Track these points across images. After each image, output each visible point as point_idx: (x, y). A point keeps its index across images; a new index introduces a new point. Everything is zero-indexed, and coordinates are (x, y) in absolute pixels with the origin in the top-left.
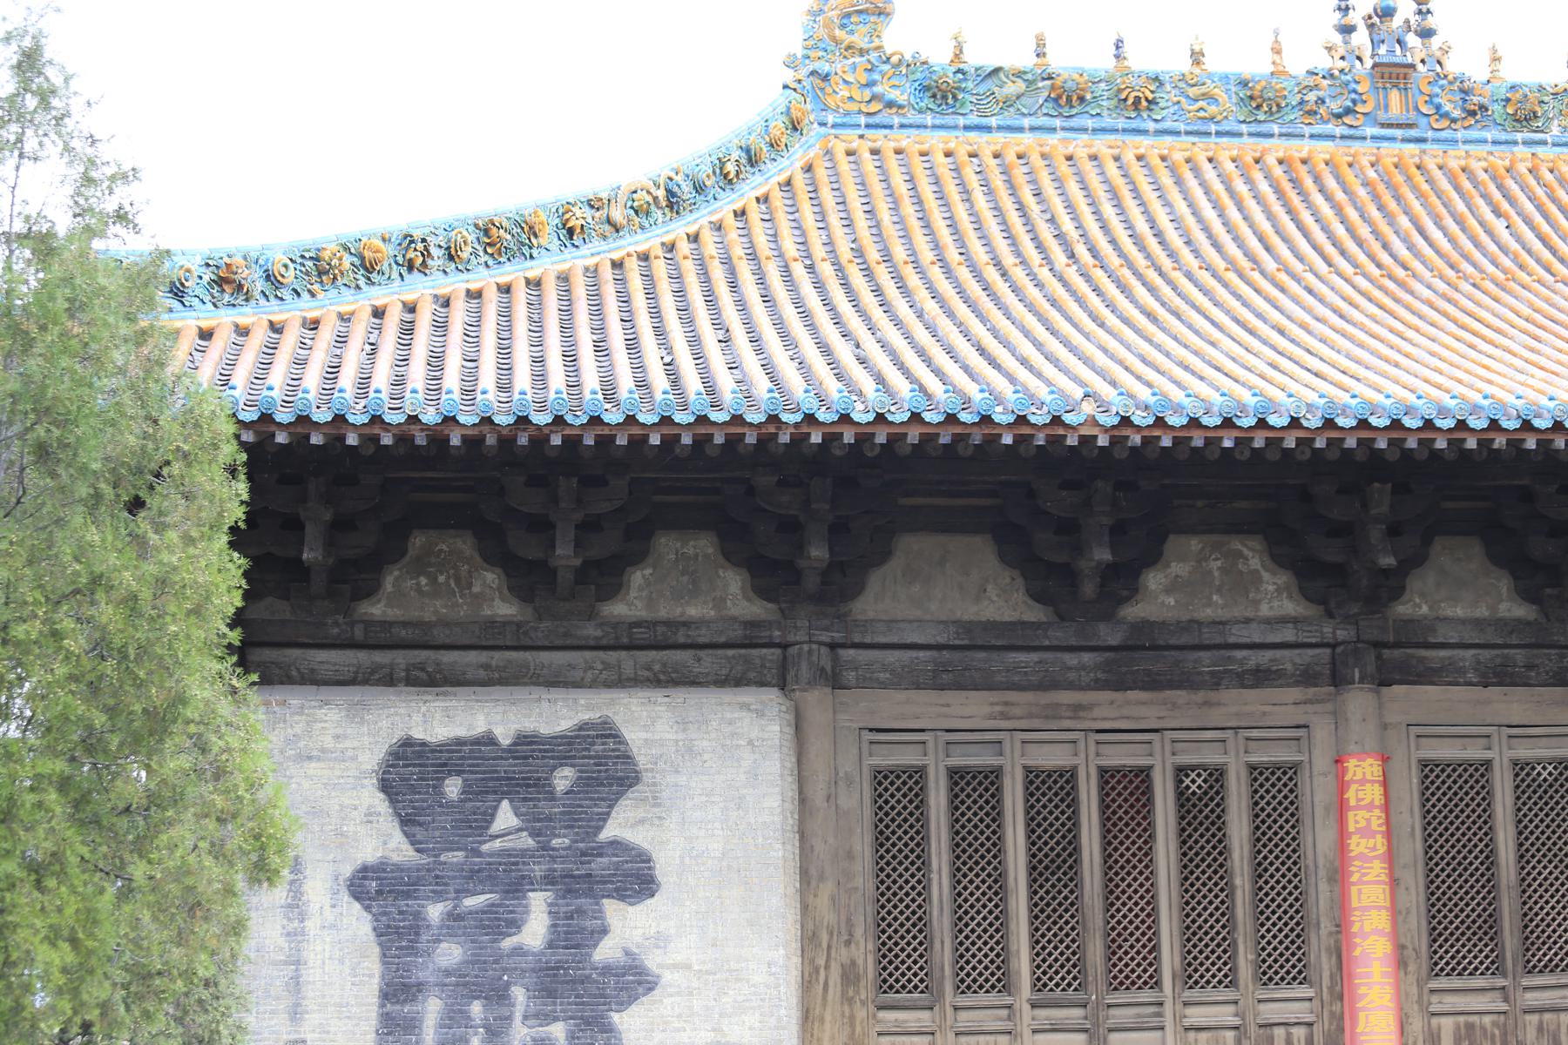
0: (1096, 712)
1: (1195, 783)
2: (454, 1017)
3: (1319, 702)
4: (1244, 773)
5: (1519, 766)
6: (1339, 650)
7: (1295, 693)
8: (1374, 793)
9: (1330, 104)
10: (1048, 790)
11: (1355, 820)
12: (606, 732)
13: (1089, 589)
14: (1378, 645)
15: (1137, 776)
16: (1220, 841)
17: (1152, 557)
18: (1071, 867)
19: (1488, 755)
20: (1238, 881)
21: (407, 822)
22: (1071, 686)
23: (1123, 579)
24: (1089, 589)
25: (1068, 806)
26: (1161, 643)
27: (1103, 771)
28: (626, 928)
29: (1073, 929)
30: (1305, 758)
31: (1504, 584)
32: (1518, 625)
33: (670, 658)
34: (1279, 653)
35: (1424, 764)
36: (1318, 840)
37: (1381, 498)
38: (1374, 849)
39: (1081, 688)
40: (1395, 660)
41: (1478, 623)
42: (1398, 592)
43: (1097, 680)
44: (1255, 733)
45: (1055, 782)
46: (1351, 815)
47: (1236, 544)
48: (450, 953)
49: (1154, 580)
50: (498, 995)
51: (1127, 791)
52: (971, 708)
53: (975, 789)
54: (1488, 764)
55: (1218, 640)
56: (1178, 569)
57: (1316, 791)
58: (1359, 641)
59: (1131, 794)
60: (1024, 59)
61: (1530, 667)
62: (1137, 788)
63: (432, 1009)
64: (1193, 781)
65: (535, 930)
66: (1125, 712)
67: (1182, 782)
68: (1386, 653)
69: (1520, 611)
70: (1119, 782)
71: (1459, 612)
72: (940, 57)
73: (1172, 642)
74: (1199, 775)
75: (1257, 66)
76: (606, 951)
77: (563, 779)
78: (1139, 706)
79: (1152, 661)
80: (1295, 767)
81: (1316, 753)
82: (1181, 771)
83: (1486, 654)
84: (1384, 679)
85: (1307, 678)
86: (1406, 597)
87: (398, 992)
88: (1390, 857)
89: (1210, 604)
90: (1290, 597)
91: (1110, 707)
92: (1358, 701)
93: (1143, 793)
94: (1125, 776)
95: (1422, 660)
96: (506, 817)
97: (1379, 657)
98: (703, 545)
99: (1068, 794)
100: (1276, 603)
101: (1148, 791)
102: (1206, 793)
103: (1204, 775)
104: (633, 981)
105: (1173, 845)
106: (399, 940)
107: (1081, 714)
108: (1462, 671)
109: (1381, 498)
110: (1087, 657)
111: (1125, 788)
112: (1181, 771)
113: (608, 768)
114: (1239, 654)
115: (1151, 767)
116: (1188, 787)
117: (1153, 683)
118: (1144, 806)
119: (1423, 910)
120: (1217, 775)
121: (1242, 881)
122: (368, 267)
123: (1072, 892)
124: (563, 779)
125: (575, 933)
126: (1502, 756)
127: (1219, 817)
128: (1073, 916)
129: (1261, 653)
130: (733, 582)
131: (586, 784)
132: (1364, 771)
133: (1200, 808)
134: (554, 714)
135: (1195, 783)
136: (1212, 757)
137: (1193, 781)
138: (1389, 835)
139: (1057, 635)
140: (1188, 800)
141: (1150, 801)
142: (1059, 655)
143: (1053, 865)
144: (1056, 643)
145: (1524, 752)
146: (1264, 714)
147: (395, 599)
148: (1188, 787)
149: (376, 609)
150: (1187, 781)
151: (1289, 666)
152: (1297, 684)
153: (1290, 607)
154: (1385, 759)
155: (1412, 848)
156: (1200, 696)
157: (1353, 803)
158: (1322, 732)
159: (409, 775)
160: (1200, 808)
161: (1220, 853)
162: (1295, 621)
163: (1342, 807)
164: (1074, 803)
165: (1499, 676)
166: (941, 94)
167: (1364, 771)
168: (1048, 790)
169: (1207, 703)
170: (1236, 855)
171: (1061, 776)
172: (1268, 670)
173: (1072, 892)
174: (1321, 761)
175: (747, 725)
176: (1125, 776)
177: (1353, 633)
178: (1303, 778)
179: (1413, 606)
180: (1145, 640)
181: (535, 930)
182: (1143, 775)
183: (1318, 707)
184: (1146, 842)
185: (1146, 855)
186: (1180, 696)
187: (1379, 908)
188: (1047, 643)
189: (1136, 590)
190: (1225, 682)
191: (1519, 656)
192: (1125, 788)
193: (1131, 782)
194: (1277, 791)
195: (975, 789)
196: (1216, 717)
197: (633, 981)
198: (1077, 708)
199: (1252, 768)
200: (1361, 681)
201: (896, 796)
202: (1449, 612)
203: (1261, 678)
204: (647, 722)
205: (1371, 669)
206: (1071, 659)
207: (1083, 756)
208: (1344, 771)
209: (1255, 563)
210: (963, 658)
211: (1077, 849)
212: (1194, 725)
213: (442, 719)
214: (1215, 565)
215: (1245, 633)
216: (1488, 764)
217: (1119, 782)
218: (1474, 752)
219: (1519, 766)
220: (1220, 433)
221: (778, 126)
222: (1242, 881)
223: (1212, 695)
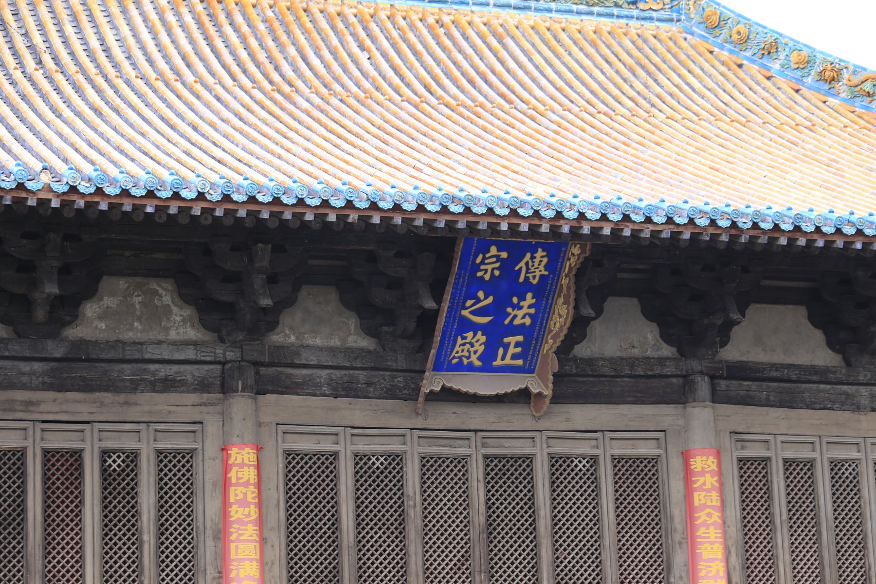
0: (43, 407)
1: (115, 463)
3: (211, 404)
4: (153, 456)
5: (359, 458)
6: (228, 366)
7: (193, 398)
8: (250, 474)
11: (235, 493)
13: (40, 314)
14: (256, 364)
15: (71, 456)
16: (133, 507)
17: (90, 292)
18: (19, 524)
19: (336, 448)
20: (145, 537)
22: (24, 387)
23: (67, 308)
24: (40, 314)
25: (19, 478)
26: (94, 356)
27: (46, 452)
29: (19, 571)
30: (199, 446)
31: (352, 322)
32: (362, 353)
34: (182, 368)
35: (288, 453)
36: (207, 508)
37: (263, 254)
38: (249, 515)
39: (31, 389)
41: (332, 350)
42: (273, 326)
43: (44, 383)
44: (162, 427)
45: (9, 459)
46: (232, 489)
47: (153, 285)
49: (90, 309)
51: (64, 467)
54: (335, 455)
55: (137, 356)
56: (109, 302)
57: (206, 471)
58: (242, 360)
59: (67, 470)
61: (369, 384)
62: (72, 465)
64: (114, 461)
66: (65, 407)
67: (106, 461)
68: (263, 370)
69: (364, 342)
70: (58, 461)
71: (318, 342)
73: (103, 356)
74: (119, 457)
78: (76, 404)
79: (88, 370)
80: (192, 453)
81: (208, 443)
82: (105, 454)
83: (337, 373)
84: (260, 389)
85: (203, 386)
86: (278, 330)
88: (261, 522)
89: (132, 329)
90: (192, 326)
91: (53, 404)
92: (240, 405)
93: (76, 470)
94: (62, 456)
95: (289, 376)
97: (257, 373)
99: (19, 469)
100: (181, 330)
101: (80, 468)
102: (123, 470)
103: (123, 457)
105: (97, 509)
107: (31, 408)
108: (319, 386)
109: (263, 254)
110: (37, 366)
111: (62, 465)
112: (105, 454)
114: (153, 367)
115: (82, 450)
116: (110, 466)
117: (86, 387)
118: (76, 479)
119: (284, 562)
120: (133, 457)
121: (149, 537)
123: (19, 543)
126: (346, 449)
127: (133, 489)
128: (19, 562)
129: (168, 367)
132: (243, 457)
133: (119, 481)
135: (115, 463)
136: (129, 443)
137: (114, 461)
138: (259, 506)
139: (15, 348)
140: (110, 475)
141: (81, 475)
142: (16, 363)
144: (13, 354)
145: (364, 446)
146: (170, 412)
148: (110, 466)
150: (110, 461)
151: (189, 377)
152: (195, 391)
153: (192, 333)
154: (259, 449)
155: (277, 515)
156: (122, 397)
157: (234, 480)
158: (212, 427)
161: (133, 516)
162: (196, 344)
163: (226, 483)
164: (23, 476)
165: (346, 390)
167: (243, 457)
169: (127, 403)
170: (145, 518)
171: (14, 455)
172: (174, 380)
173: (19, 543)
174: (211, 448)
176: (62, 456)
177: (238, 354)
178: (197, 461)
179: (285, 335)
180: (83, 354)
182: (77, 455)
183: (210, 409)
184: (77, 506)
185: (76, 516)
186: (108, 397)
187: (251, 560)
188: (7, 354)
189: (77, 317)
190: (141, 387)
191: (361, 375)
192: (62, 465)
193: (67, 461)
194: (178, 469)
196: (133, 413)
198: (29, 403)
199: (159, 452)
200: (243, 390)
202: (311, 342)
203: (168, 385)
205: (251, 381)
206: (25, 367)
207: (31, 440)
208: (228, 457)
209: (167, 299)
211: (24, 511)
212: (116, 419)
214: (137, 300)
215: (157, 351)
216: (335, 455)
217: (58, 461)
218: (326, 446)
219: (359, 458)
220: (144, 202)
222: (149, 537)
223: (132, 398)
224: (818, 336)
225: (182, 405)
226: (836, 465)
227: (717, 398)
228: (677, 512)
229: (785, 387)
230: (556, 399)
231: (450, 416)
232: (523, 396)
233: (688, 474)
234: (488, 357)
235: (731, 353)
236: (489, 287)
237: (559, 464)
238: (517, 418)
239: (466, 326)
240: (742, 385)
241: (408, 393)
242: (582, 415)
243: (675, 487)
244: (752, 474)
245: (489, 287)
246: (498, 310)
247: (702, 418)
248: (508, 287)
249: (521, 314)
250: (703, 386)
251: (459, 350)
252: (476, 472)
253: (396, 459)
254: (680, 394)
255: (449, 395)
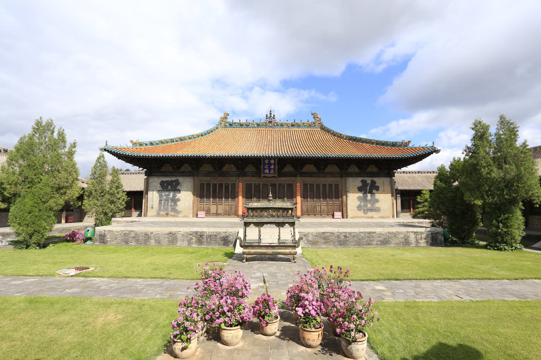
2: (165, 202)
9: (265, 125)
10: (215, 185)
12: (178, 180)
17: (224, 166)
21: (162, 187)
28: (178, 195)
31: (254, 168)
33: (184, 174)
36: (237, 189)
37: (240, 162)
40: (244, 175)
48: (165, 197)
49: (224, 168)
50: (168, 201)
51: (221, 185)
52: (208, 178)
53: (209, 185)
57: (237, 186)
60: (238, 122)
63: (163, 202)
65: (171, 196)
72: (231, 122)
75: (258, 122)
76: (177, 198)
77: (174, 184)
84: (243, 176)
85: (236, 176)
87: (160, 200)
91: (220, 178)
92: (241, 178)
96: (169, 187)
98: (188, 165)
104: (179, 200)
106: (161, 196)
109: (240, 162)
113: (178, 183)
122: (167, 142)
124: (174, 184)
125: (174, 196)
126: (253, 183)
130: (190, 168)
131: (176, 184)
132: (241, 185)
133: (227, 187)
134: (174, 179)
143: (215, 191)
147: (163, 169)
149: (162, 170)
155: (245, 191)
158: (237, 181)
159: (162, 183)
160: (227, 187)
165: (254, 176)
166: (231, 125)
168: (215, 185)
175: (189, 180)
179: (246, 170)
181: (171, 196)
195: (209, 185)
197: (179, 200)
201: (202, 185)
203: (232, 176)
204: (181, 179)
210: (208, 174)
213: (165, 179)
221: (215, 128)
224: (315, 168)
225: (234, 178)
226: (317, 184)
227: (301, 176)
228: (295, 190)
229: (310, 175)
230: (279, 176)
231: (265, 179)
232: (274, 177)
233: (296, 186)
234: (269, 172)
235: (303, 171)
236: (267, 164)
237: (280, 184)
238: (274, 179)
239: (266, 169)
240: (304, 174)
241: (259, 176)
242: (283, 179)
243: (295, 187)
244: (305, 186)
245: (267, 164)
246: (269, 167)
247: (299, 178)
248: (270, 164)
249: (272, 167)
250: (299, 175)
251: (266, 171)
252: (269, 185)
253: (259, 184)
254: (296, 176)
255: (264, 177)
